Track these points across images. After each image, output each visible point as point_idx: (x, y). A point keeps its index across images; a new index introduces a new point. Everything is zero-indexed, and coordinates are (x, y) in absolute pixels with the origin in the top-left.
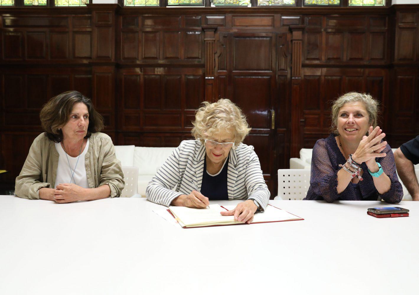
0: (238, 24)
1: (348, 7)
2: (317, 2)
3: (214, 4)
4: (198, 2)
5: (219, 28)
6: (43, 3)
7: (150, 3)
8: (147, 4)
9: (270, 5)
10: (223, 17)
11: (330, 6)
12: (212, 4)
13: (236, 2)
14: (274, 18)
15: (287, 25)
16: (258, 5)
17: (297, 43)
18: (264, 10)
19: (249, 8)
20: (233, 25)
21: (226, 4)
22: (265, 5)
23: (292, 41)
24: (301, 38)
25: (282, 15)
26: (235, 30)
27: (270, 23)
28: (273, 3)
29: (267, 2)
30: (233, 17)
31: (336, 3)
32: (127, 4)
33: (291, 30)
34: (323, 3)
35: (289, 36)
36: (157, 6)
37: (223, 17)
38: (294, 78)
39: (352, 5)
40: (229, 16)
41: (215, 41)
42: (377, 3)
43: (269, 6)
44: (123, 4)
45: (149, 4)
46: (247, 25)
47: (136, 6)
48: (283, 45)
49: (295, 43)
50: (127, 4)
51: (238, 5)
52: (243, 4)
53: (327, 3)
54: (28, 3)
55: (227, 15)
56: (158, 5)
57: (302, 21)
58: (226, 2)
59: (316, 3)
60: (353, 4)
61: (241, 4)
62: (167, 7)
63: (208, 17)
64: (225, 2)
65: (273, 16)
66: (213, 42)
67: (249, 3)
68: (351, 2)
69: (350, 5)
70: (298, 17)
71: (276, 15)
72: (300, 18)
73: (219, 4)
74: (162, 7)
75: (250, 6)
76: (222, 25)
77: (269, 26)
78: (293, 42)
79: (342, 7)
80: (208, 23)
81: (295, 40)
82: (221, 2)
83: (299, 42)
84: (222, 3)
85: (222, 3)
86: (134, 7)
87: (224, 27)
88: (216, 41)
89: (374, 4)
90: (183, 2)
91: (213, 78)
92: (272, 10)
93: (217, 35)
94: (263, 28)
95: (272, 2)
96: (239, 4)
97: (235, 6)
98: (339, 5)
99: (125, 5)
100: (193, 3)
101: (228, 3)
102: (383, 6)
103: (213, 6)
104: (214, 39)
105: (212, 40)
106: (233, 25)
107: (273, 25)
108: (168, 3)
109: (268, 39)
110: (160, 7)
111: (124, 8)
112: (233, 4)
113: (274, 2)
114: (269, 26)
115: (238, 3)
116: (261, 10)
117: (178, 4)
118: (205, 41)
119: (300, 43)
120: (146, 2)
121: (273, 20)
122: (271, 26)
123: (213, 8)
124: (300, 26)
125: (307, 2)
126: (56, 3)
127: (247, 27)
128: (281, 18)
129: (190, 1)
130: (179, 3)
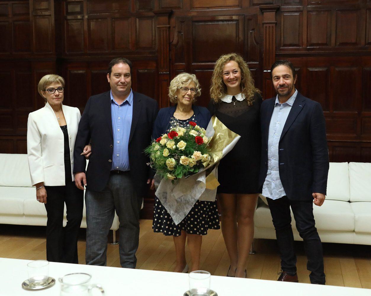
5: (173, 10)
17: (269, 27)
20: (192, 7)
27: (237, 3)
33: (262, 10)
38: (266, 71)
41: (169, 27)
48: (253, 29)
49: (266, 27)
77: (234, 6)
83: (271, 25)
93: (173, 20)
104: (169, 26)
105: (166, 27)
109: (234, 23)
114: (234, 6)
119: (273, 27)
122: (239, 6)
124: (275, 5)
127: (208, 9)
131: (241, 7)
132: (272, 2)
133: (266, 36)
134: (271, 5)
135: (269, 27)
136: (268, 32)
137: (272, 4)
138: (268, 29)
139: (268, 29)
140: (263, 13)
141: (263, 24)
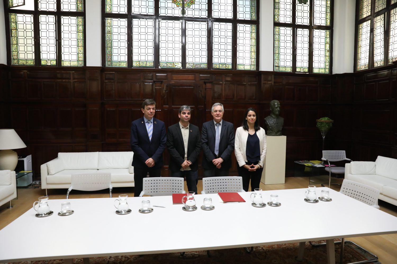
0: (175, 79)
2: (219, 67)
6: (54, 64)
7: (122, 65)
10: (166, 75)
11: (226, 69)
12: (159, 67)
15: (203, 80)
16: (186, 68)
18: (190, 71)
23: (206, 89)
26: (173, 82)
28: (195, 67)
31: (230, 68)
33: (205, 83)
37: (166, 75)
41: (161, 88)
43: (192, 68)
44: (105, 65)
48: (201, 91)
52: (178, 67)
54: (44, 64)
55: (168, 73)
61: (176, 67)
63: (157, 74)
65: (195, 74)
67: (181, 67)
77: (192, 80)
78: (207, 89)
79: (233, 71)
80: (157, 78)
81: (207, 89)
84: (165, 67)
87: (167, 80)
91: (160, 110)
95: (194, 66)
108: (133, 66)
112: (171, 67)
115: (174, 66)
118: (155, 88)
122: (194, 80)
126: (62, 64)
131: (195, 80)
137: (209, 80)
140: (206, 84)
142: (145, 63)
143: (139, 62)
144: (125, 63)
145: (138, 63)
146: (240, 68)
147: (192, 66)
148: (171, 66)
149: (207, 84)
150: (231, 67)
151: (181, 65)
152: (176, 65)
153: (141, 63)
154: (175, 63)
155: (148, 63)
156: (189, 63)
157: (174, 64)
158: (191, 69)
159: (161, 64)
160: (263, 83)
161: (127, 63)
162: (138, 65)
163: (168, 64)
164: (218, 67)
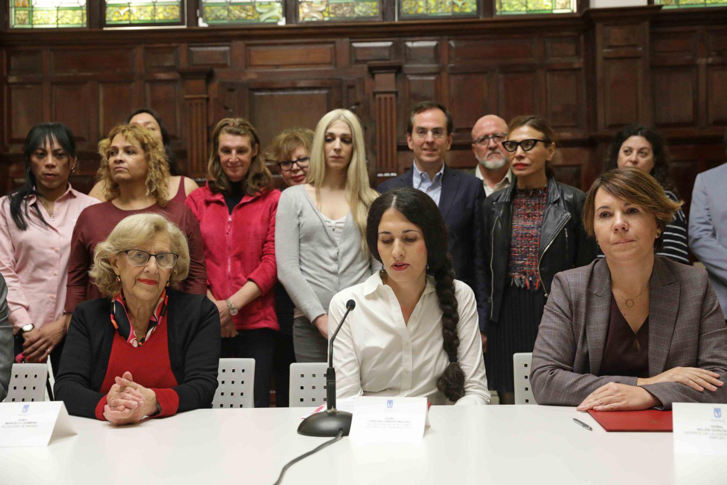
1: (494, 18)
2: (427, 9)
3: (205, 20)
4: (171, 18)
5: (216, 70)
7: (68, 21)
8: (60, 22)
9: (326, 19)
10: (227, 48)
11: (455, 16)
12: (200, 20)
13: (253, 16)
14: (335, 48)
16: (301, 19)
17: (386, 99)
19: (282, 28)
20: (248, 65)
21: (231, 20)
22: (314, 19)
24: (393, 89)
25: (352, 40)
26: (251, 75)
27: (328, 58)
28: (332, 16)
29: (320, 14)
30: (247, 48)
31: (468, 10)
32: (15, 24)
33: (373, 71)
34: (440, 10)
35: (368, 82)
36: (82, 28)
39: (504, 13)
40: (239, 44)
41: (208, 99)
42: (558, 6)
43: (323, 21)
45: (64, 22)
46: (276, 63)
47: (35, 26)
49: (380, 99)
50: (15, 24)
51: (256, 21)
52: (268, 18)
53: (450, 10)
56: (85, 26)
57: (398, 49)
58: (232, 17)
59: (425, 12)
60: (505, 11)
61: (263, 18)
62: (105, 29)
64: (228, 16)
65: (333, 43)
66: (204, 102)
67: (280, 16)
68: (501, 7)
69: (498, 13)
70: (389, 44)
71: (338, 40)
72: (392, 45)
73: (216, 20)
74: (92, 30)
75: (282, 23)
76: (224, 66)
78: (377, 96)
79: (481, 18)
82: (221, 15)
83: (388, 96)
84: (223, 19)
85: (222, 17)
86: (32, 29)
88: (211, 100)
89: (552, 10)
90: (138, 18)
92: (330, 30)
93: (214, 86)
94: (312, 69)
95: (329, 13)
96: (258, 19)
97: (251, 24)
98: (475, 14)
99: (11, 27)
100: (160, 20)
101: (234, 17)
102: (573, 13)
103: (202, 24)
104: (205, 96)
106: (248, 65)
107: (334, 62)
110: (88, 29)
111: (8, 31)
112: (245, 19)
113: (333, 13)
116: (305, 31)
117: (127, 22)
120: (58, 20)
121: (335, 53)
122: (330, 64)
123: (203, 30)
124: (394, 61)
125: (406, 10)
128: (351, 46)
129: (155, 16)
130: (129, 20)
131: (336, 65)
132: (387, 58)
133: (380, 116)
134: (388, 62)
135: (386, 99)
136: (383, 106)
138: (383, 101)
139: (383, 101)
140: (373, 76)
141: (375, 94)
142: (150, 9)
143: (129, 6)
144: (79, 12)
145: (123, 11)
146: (507, 9)
147: (321, 12)
148: (243, 15)
149: (377, 77)
150: (475, 7)
151: (281, 10)
152: (261, 13)
153: (134, 10)
154: (257, 5)
155: (160, 10)
156: (312, 2)
157: (254, 7)
158: (318, 22)
159: (207, 9)
160: (606, 59)
161: (85, 12)
162: (126, 17)
163: (231, 8)
164: (421, 10)
